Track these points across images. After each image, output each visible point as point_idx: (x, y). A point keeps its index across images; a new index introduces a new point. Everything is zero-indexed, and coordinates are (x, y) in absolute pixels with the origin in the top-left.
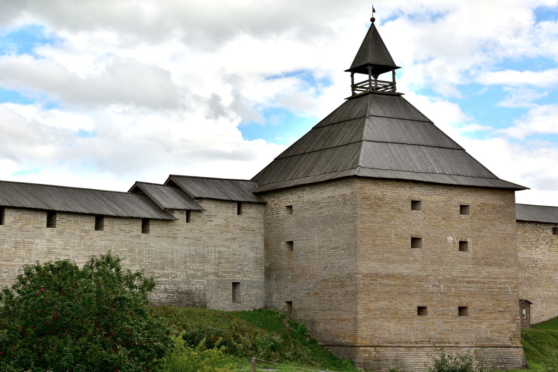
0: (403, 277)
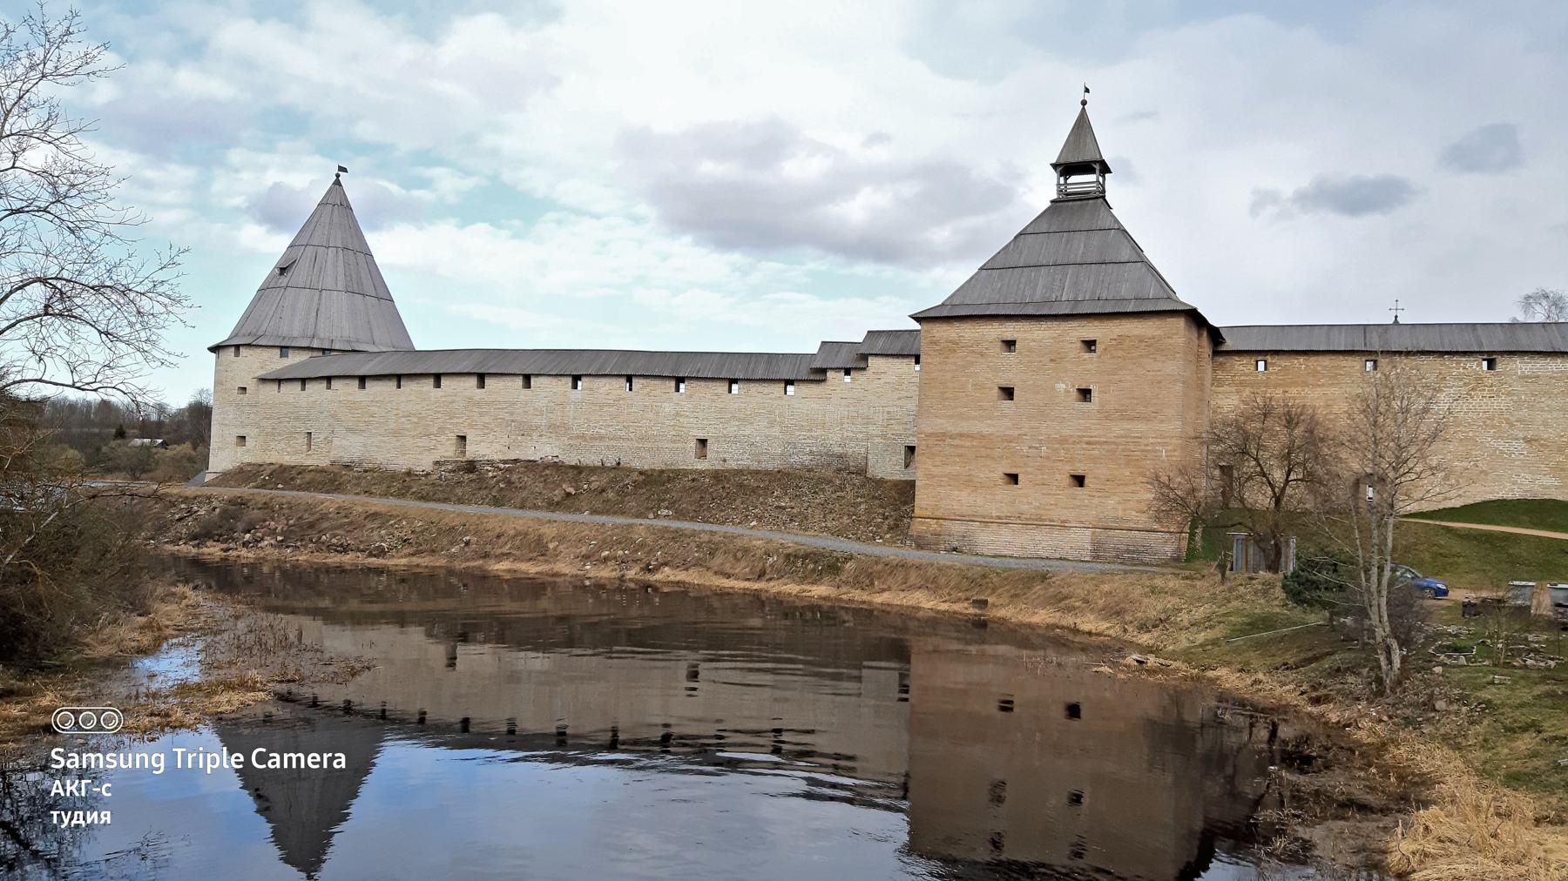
0: (983, 437)
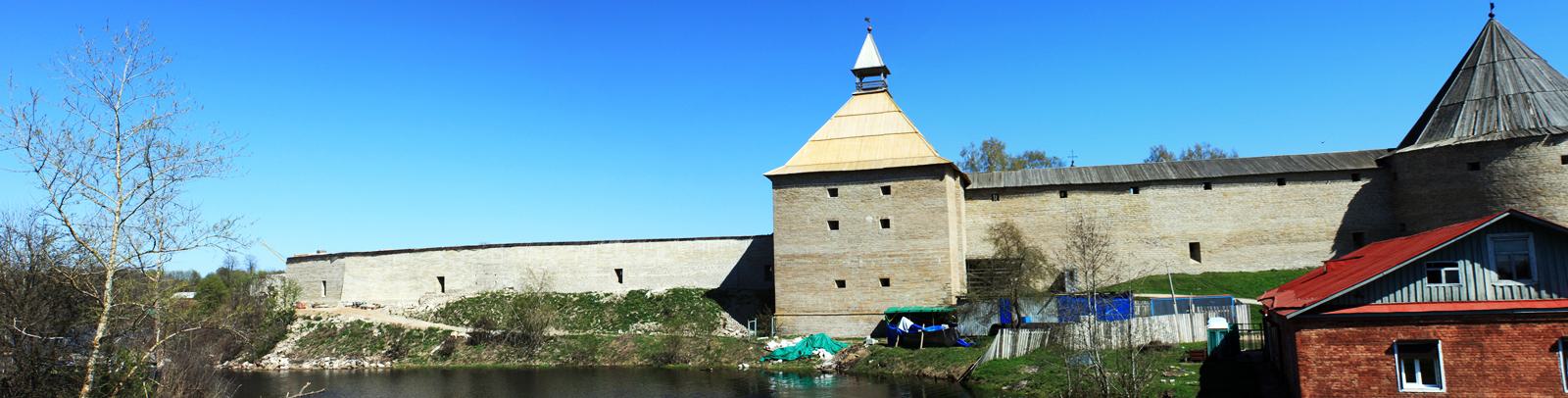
0: (820, 256)
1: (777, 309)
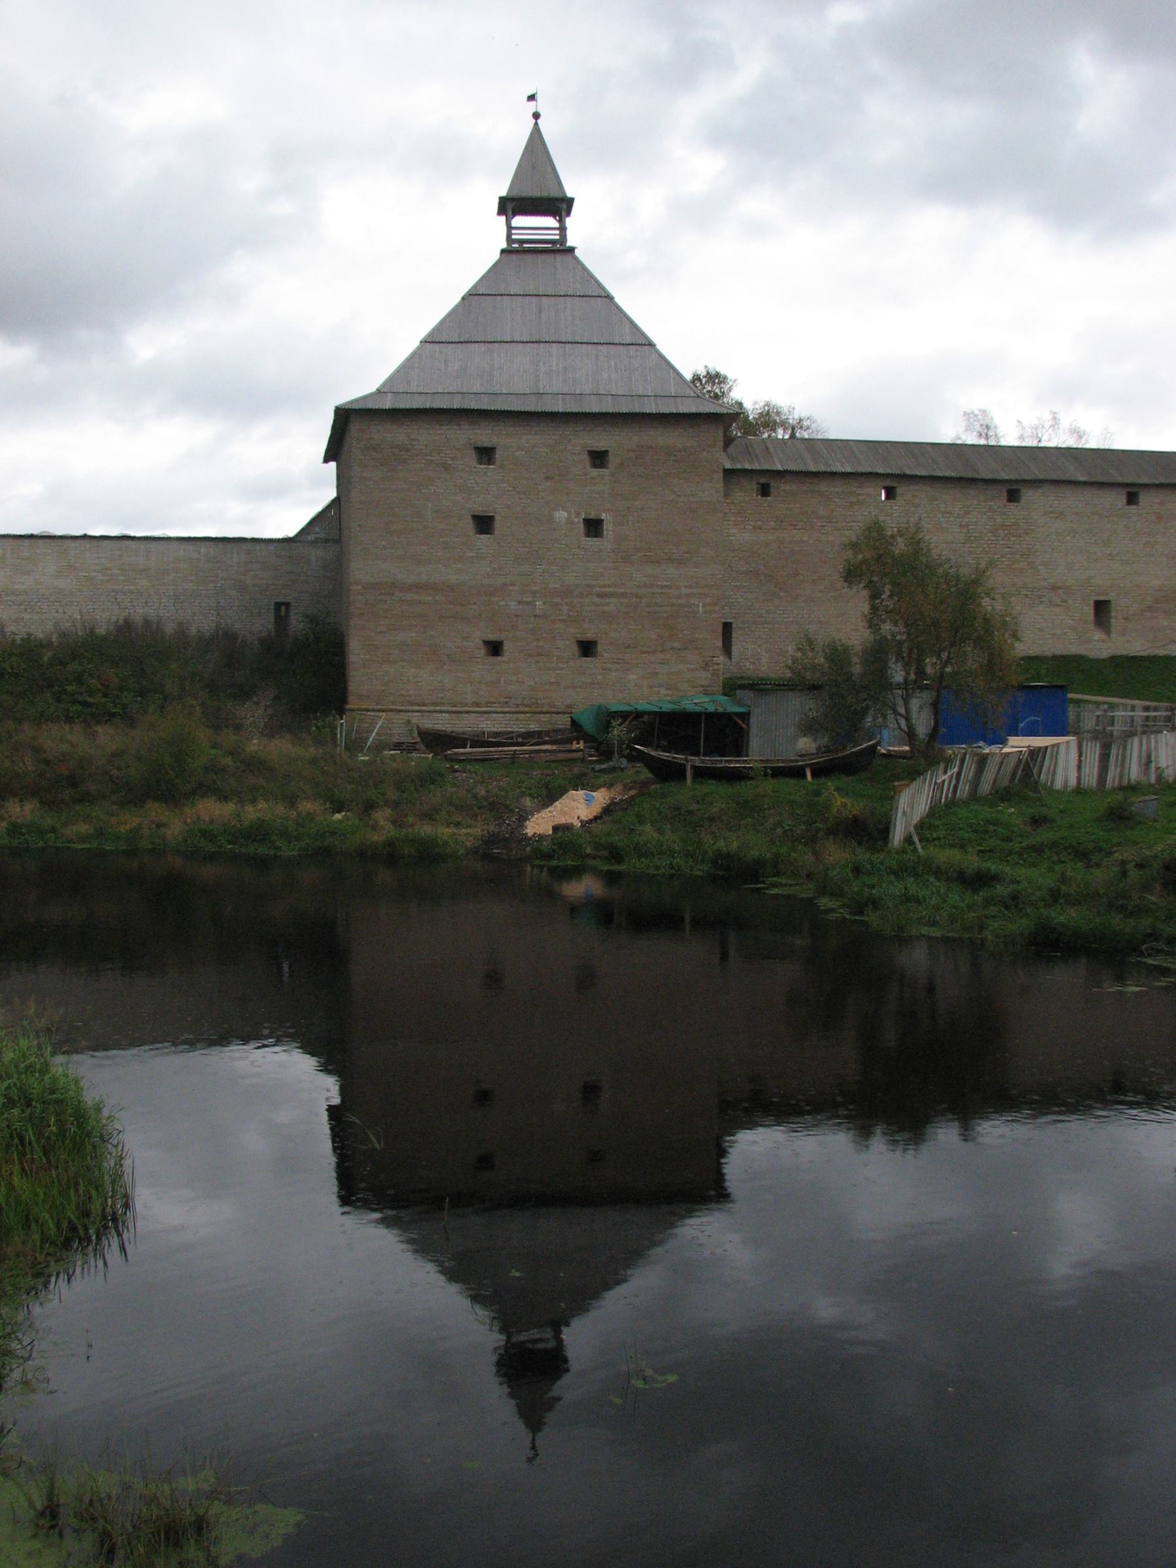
1: (352, 698)
